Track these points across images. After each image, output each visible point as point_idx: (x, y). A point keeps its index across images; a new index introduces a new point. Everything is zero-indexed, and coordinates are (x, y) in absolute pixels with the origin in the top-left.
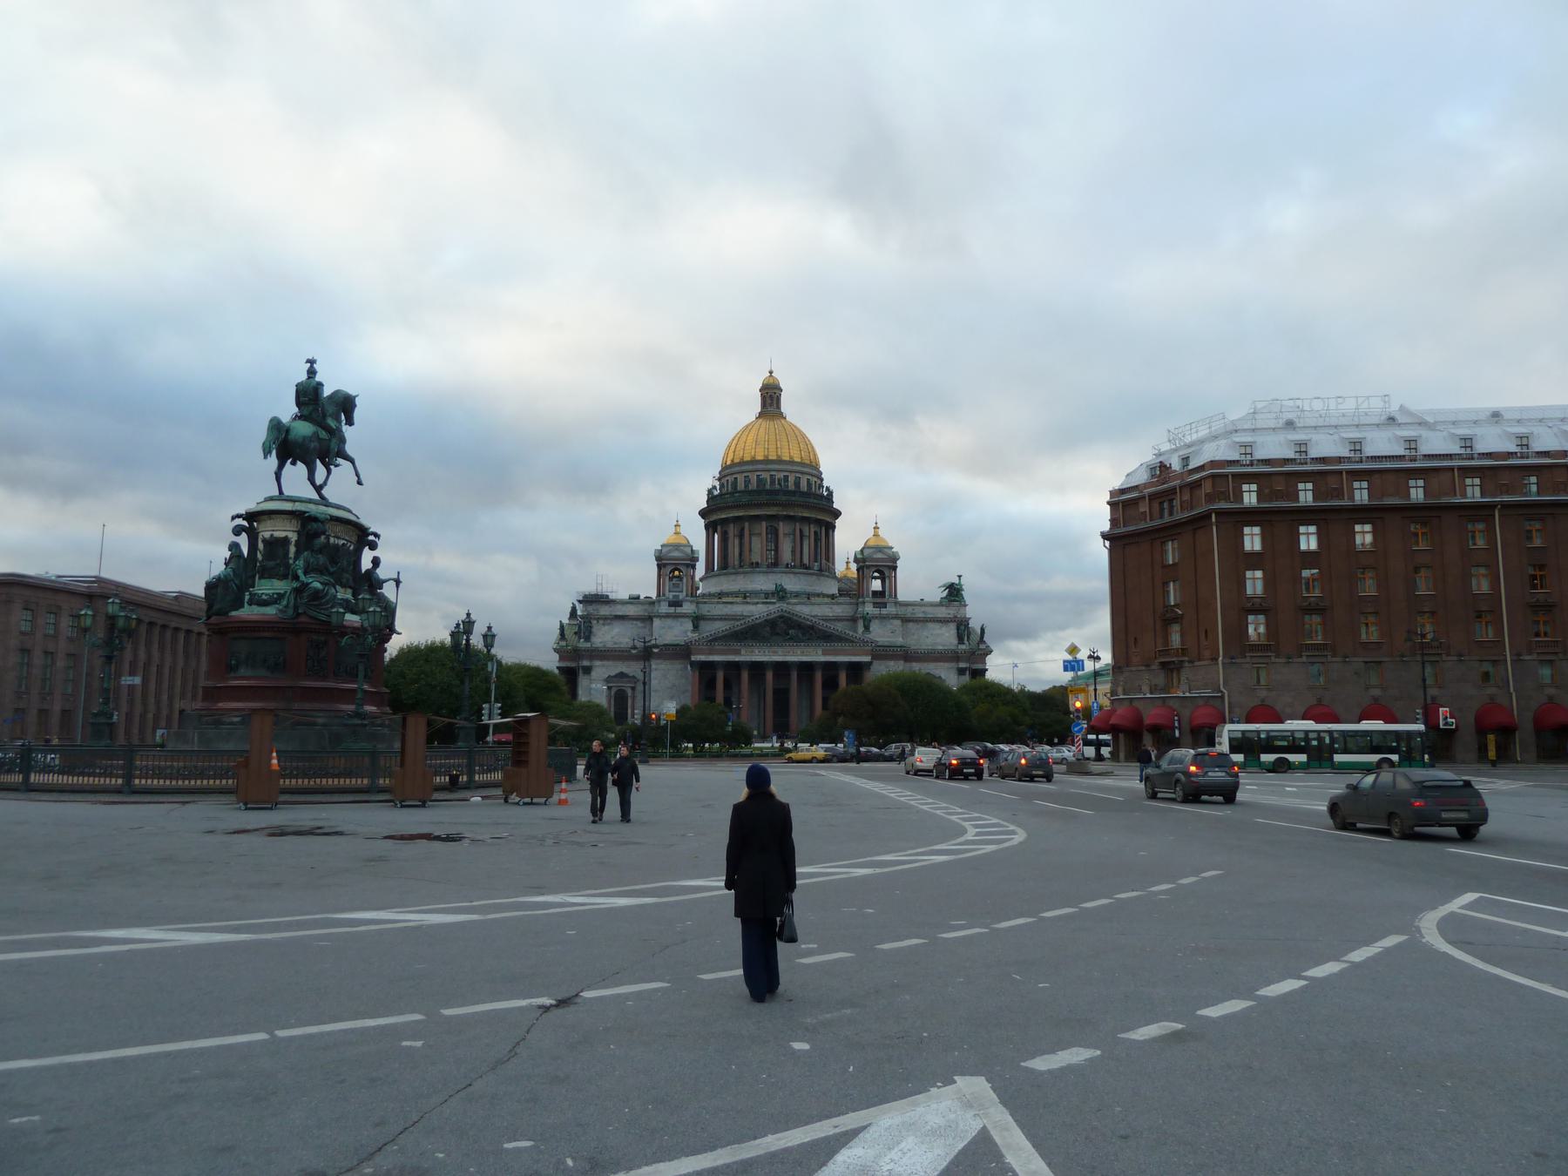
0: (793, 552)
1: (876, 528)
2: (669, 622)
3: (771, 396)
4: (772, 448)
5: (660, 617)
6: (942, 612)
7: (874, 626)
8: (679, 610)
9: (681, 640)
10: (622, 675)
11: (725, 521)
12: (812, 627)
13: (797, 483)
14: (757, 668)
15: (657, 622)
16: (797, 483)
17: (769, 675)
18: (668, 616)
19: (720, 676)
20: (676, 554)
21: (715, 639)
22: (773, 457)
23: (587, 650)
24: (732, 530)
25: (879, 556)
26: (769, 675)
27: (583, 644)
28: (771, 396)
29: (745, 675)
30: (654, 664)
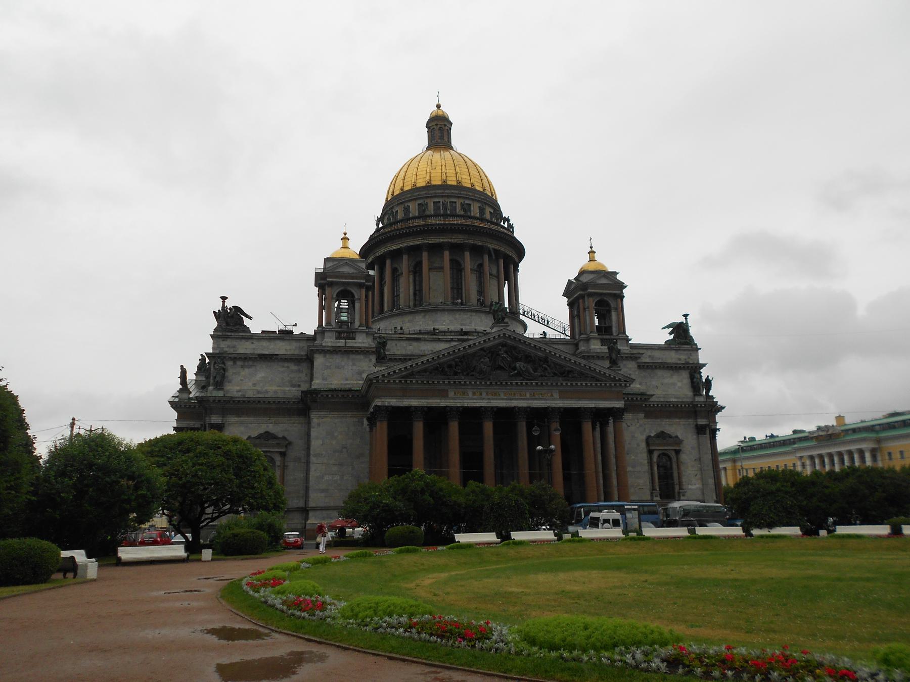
0: (481, 292)
1: (592, 253)
2: (337, 359)
3: (439, 130)
4: (451, 171)
5: (325, 351)
6: (672, 357)
7: (621, 364)
8: (350, 343)
9: (357, 383)
10: (267, 436)
11: (396, 255)
12: (546, 360)
13: (482, 211)
14: (471, 417)
15: (319, 360)
16: (482, 211)
17: (488, 427)
18: (335, 351)
19: (419, 428)
20: (346, 269)
21: (412, 375)
22: (452, 182)
23: (218, 401)
24: (405, 264)
25: (604, 281)
26: (488, 427)
27: (212, 392)
28: (439, 130)
29: (454, 427)
30: (316, 417)
